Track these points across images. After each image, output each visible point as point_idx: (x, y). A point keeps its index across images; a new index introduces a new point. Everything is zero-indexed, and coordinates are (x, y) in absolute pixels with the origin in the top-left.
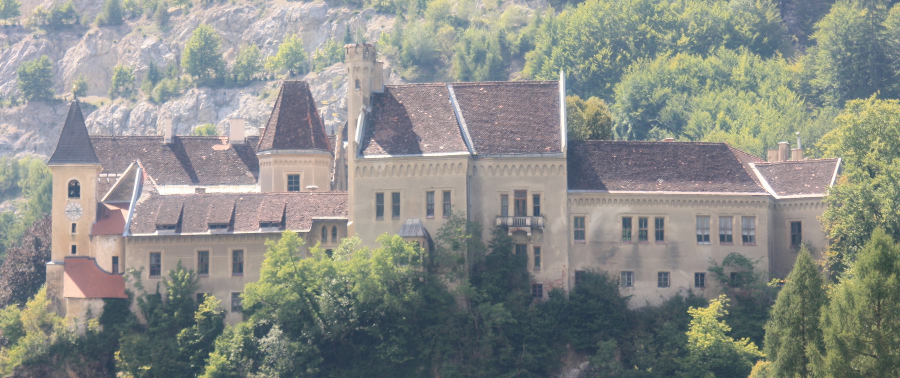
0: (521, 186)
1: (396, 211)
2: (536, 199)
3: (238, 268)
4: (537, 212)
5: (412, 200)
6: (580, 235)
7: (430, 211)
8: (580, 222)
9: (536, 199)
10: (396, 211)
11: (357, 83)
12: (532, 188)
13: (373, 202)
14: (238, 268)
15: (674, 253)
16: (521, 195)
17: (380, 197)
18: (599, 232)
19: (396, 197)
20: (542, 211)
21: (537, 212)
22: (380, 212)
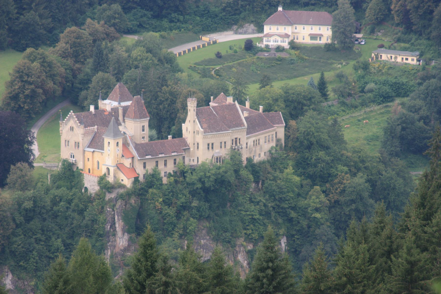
0: (236, 137)
1: (212, 148)
2: (239, 139)
3: (165, 165)
4: (239, 142)
5: (217, 145)
6: (247, 147)
7: (221, 147)
8: (247, 144)
9: (239, 139)
10: (212, 148)
11: (194, 110)
12: (239, 137)
13: (207, 146)
14: (165, 165)
15: (261, 148)
16: (236, 139)
17: (208, 145)
18: (250, 146)
19: (213, 144)
20: (241, 143)
21: (239, 142)
22: (208, 148)
